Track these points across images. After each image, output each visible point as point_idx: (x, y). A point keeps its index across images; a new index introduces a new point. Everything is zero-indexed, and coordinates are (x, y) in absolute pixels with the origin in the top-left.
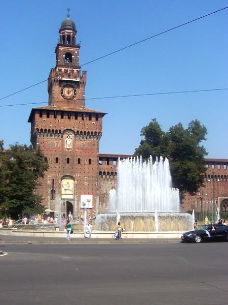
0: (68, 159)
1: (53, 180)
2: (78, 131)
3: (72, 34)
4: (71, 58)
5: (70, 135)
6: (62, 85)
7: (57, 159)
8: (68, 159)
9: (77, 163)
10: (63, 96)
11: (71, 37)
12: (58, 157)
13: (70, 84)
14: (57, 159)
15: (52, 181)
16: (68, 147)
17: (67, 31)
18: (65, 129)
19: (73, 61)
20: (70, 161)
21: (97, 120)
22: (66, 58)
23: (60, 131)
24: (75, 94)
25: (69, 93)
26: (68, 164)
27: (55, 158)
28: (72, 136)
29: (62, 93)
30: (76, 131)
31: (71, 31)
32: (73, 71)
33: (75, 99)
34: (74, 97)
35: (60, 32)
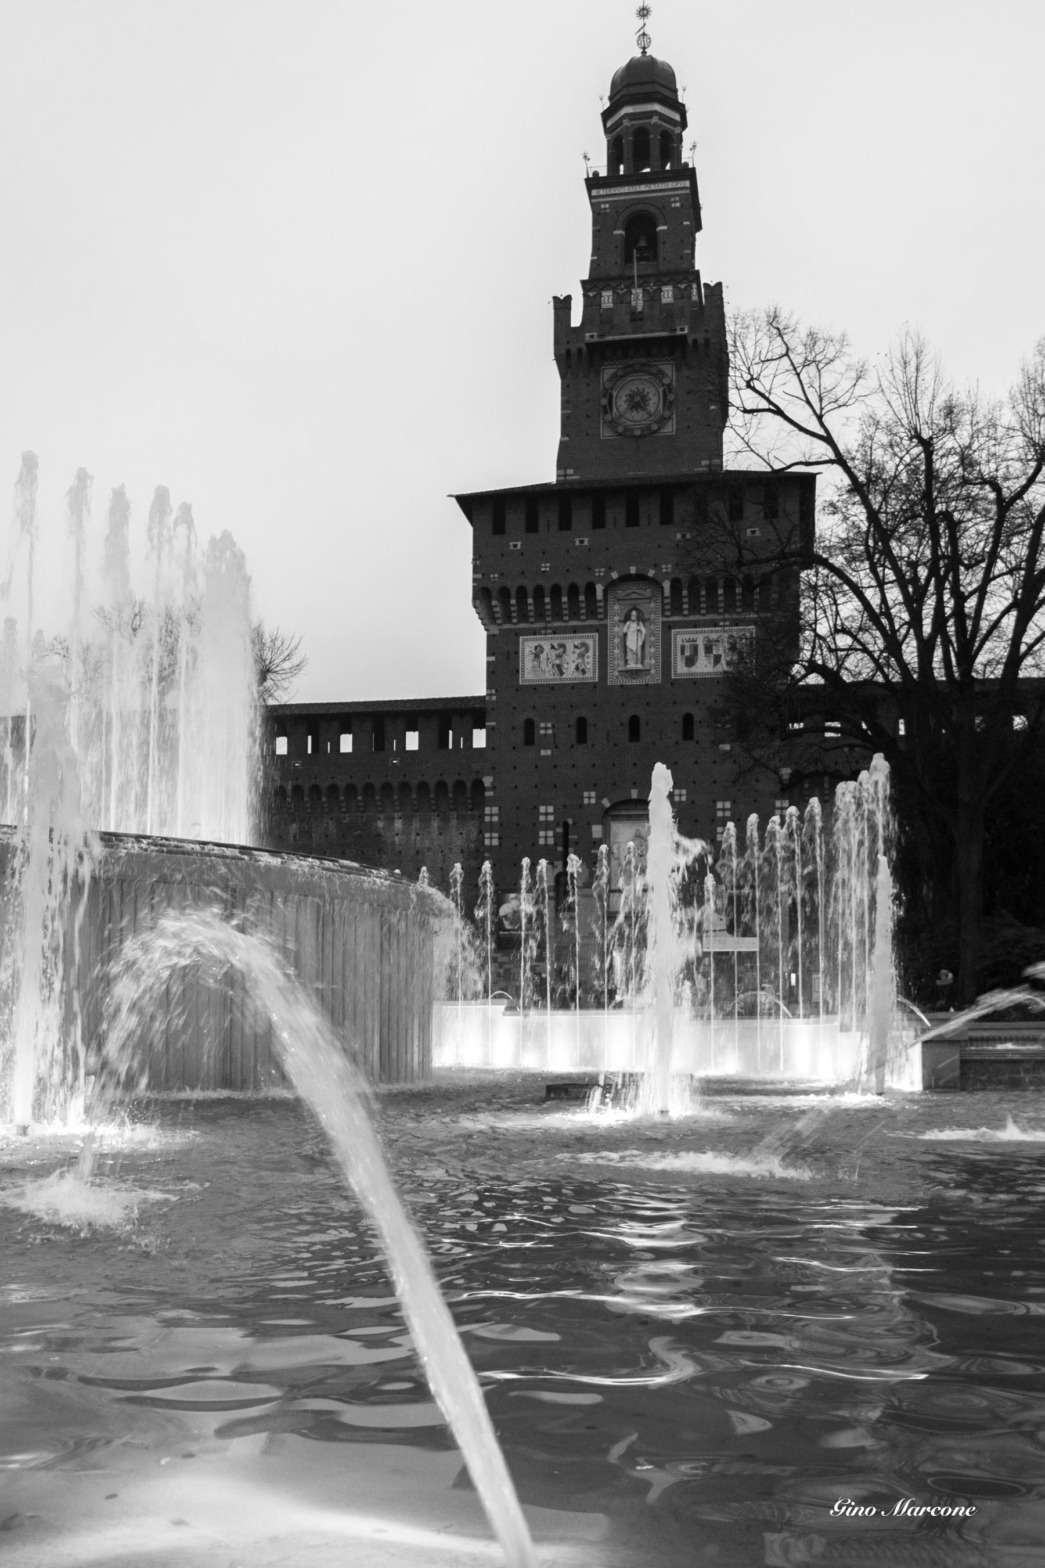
0: (634, 722)
1: (566, 825)
2: (676, 585)
3: (655, 120)
4: (655, 234)
5: (643, 606)
6: (607, 373)
7: (582, 725)
8: (634, 722)
9: (679, 736)
10: (612, 424)
11: (655, 138)
12: (584, 713)
13: (644, 360)
14: (582, 725)
15: (560, 830)
16: (632, 665)
17: (628, 110)
18: (615, 575)
19: (664, 251)
20: (643, 730)
21: (771, 513)
22: (630, 242)
23: (591, 588)
24: (668, 405)
25: (637, 402)
26: (634, 744)
27: (573, 721)
28: (652, 607)
29: (608, 409)
30: (667, 585)
31: (657, 107)
32: (653, 298)
33: (669, 429)
34: (662, 421)
35: (607, 131)
